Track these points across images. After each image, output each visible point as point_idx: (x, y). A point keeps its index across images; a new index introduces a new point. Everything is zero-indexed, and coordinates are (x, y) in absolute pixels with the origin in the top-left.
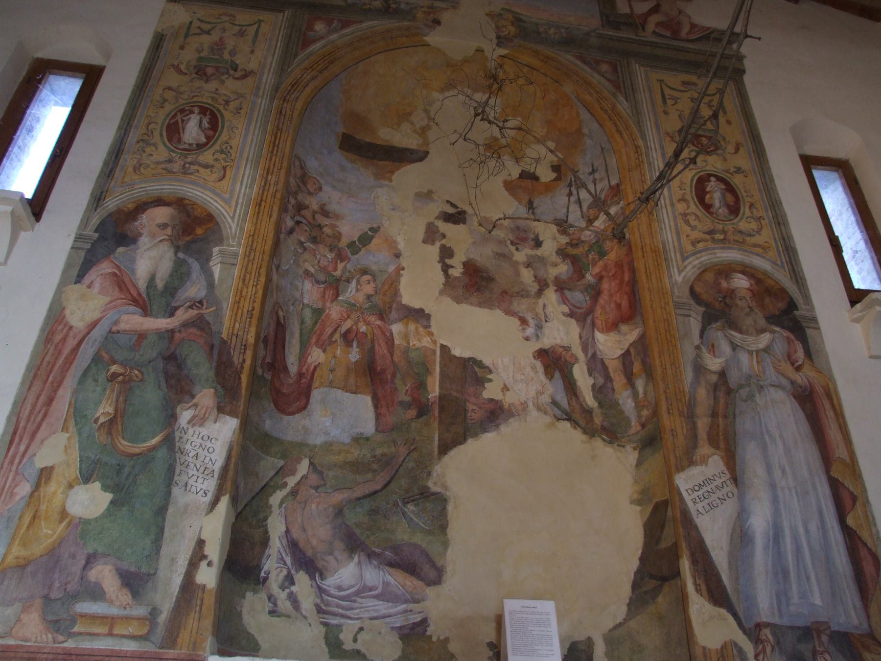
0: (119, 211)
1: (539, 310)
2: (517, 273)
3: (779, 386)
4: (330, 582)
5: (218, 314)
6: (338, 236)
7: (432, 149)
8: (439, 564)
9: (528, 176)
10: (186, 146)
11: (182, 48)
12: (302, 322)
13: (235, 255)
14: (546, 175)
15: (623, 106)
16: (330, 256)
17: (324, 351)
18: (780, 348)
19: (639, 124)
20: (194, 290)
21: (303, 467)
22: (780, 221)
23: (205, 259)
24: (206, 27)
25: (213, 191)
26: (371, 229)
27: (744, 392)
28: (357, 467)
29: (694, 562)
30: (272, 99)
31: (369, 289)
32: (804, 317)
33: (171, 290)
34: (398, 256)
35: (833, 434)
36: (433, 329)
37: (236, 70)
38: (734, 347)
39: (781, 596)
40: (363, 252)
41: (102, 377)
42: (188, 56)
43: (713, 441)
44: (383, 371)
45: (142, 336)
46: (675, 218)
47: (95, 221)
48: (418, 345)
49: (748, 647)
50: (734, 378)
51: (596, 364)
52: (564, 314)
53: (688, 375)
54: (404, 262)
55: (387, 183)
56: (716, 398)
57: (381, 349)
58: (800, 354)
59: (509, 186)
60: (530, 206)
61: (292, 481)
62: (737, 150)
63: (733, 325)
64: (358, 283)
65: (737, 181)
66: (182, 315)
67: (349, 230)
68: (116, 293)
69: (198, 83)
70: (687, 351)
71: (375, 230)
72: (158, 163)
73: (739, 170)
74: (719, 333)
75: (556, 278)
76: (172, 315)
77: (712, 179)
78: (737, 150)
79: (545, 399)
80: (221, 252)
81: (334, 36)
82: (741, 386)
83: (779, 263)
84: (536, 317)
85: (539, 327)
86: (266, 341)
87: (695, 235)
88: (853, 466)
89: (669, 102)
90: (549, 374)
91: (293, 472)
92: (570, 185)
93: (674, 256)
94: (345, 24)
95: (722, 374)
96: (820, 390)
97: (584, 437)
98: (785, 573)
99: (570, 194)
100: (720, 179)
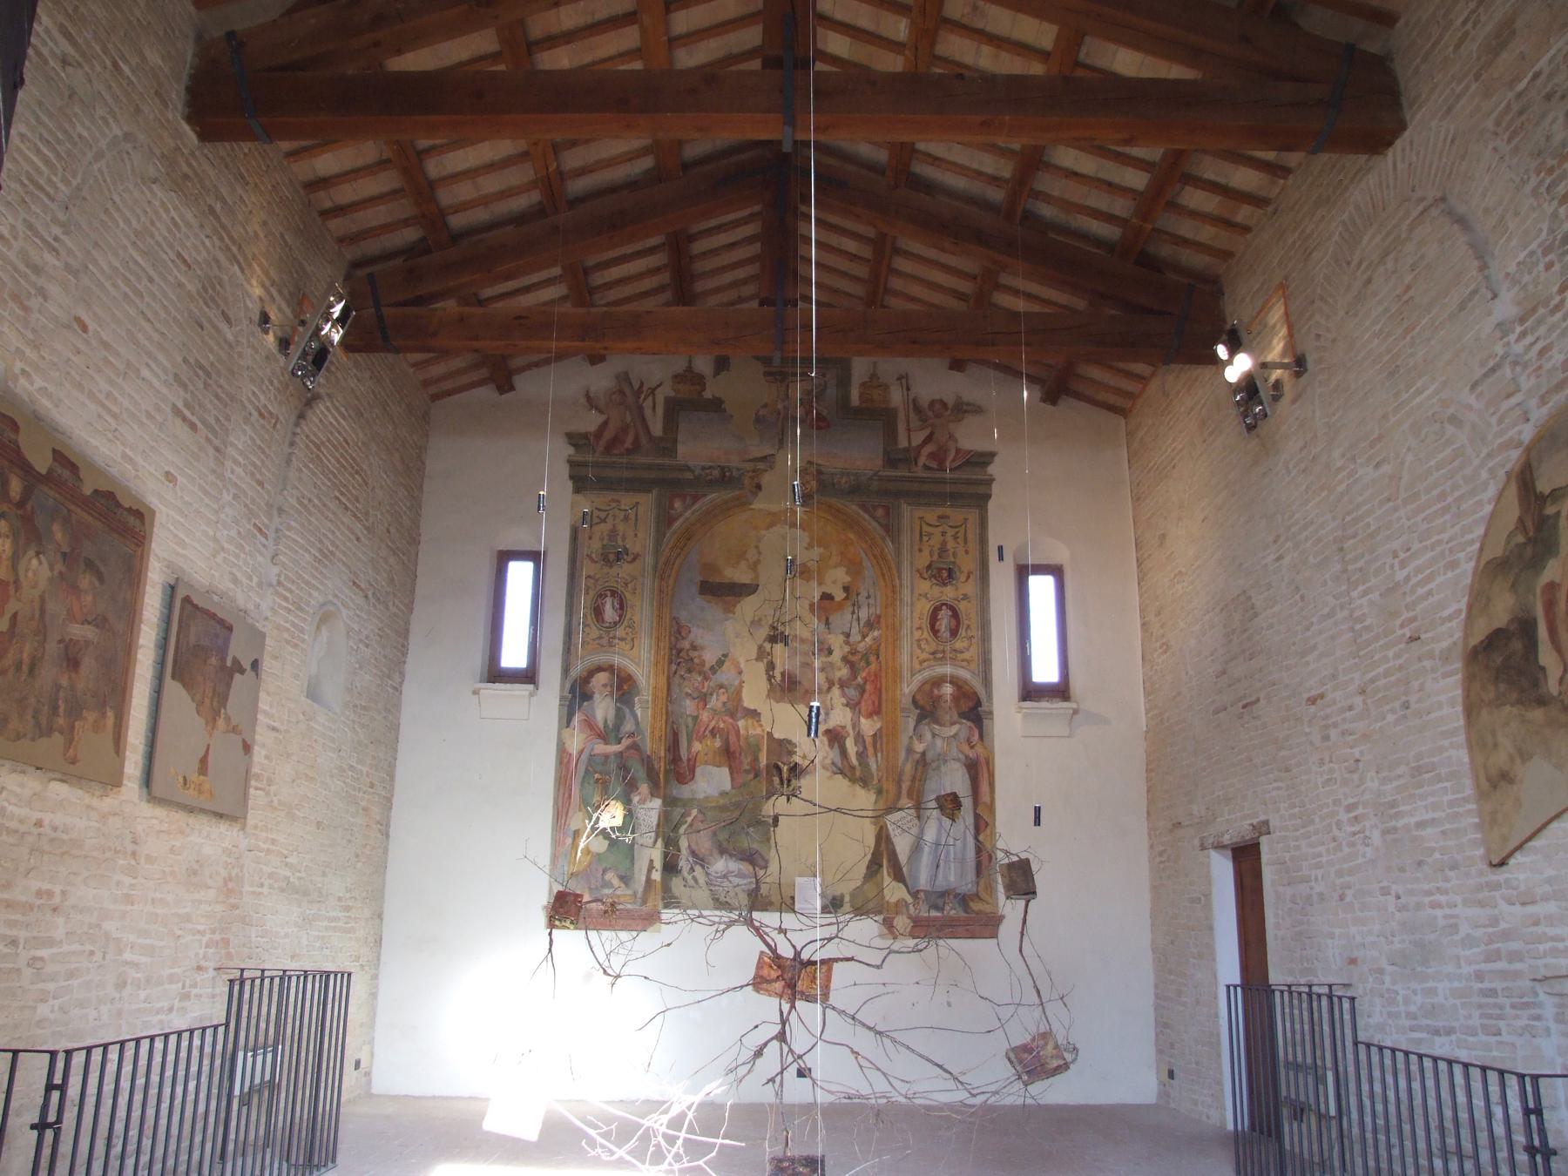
1: (828, 702)
3: (958, 760)
4: (712, 870)
6: (703, 663)
7: (762, 581)
8: (767, 858)
9: (827, 597)
10: (608, 625)
11: (590, 538)
12: (687, 727)
14: (839, 595)
15: (889, 547)
16: (699, 679)
17: (701, 742)
18: (964, 734)
20: (629, 726)
21: (694, 812)
22: (985, 638)
23: (631, 705)
24: (603, 515)
25: (629, 658)
26: (723, 655)
27: (934, 765)
28: (723, 809)
29: (889, 861)
30: (654, 577)
31: (724, 698)
32: (985, 712)
33: (617, 727)
34: (740, 673)
35: (984, 787)
36: (762, 723)
37: (627, 554)
38: (934, 735)
40: (719, 672)
41: (592, 781)
42: (596, 545)
43: (910, 796)
44: (734, 752)
45: (607, 756)
46: (912, 644)
47: (568, 686)
48: (754, 733)
49: (909, 899)
50: (929, 756)
51: (859, 738)
52: (843, 705)
53: (903, 755)
54: (745, 677)
55: (731, 615)
57: (732, 738)
60: (827, 623)
61: (689, 819)
62: (968, 577)
63: (938, 722)
64: (717, 695)
65: (962, 607)
66: (626, 742)
67: (710, 657)
69: (606, 569)
71: (725, 656)
72: (594, 640)
73: (965, 597)
74: (926, 727)
75: (840, 679)
77: (944, 607)
78: (968, 577)
79: (828, 761)
81: (688, 514)
82: (933, 761)
83: (976, 672)
87: (924, 656)
88: (991, 808)
89: (925, 539)
90: (831, 747)
91: (689, 815)
92: (854, 605)
93: (906, 674)
94: (696, 499)
95: (923, 754)
96: (982, 760)
97: (849, 784)
99: (853, 613)
100: (952, 608)
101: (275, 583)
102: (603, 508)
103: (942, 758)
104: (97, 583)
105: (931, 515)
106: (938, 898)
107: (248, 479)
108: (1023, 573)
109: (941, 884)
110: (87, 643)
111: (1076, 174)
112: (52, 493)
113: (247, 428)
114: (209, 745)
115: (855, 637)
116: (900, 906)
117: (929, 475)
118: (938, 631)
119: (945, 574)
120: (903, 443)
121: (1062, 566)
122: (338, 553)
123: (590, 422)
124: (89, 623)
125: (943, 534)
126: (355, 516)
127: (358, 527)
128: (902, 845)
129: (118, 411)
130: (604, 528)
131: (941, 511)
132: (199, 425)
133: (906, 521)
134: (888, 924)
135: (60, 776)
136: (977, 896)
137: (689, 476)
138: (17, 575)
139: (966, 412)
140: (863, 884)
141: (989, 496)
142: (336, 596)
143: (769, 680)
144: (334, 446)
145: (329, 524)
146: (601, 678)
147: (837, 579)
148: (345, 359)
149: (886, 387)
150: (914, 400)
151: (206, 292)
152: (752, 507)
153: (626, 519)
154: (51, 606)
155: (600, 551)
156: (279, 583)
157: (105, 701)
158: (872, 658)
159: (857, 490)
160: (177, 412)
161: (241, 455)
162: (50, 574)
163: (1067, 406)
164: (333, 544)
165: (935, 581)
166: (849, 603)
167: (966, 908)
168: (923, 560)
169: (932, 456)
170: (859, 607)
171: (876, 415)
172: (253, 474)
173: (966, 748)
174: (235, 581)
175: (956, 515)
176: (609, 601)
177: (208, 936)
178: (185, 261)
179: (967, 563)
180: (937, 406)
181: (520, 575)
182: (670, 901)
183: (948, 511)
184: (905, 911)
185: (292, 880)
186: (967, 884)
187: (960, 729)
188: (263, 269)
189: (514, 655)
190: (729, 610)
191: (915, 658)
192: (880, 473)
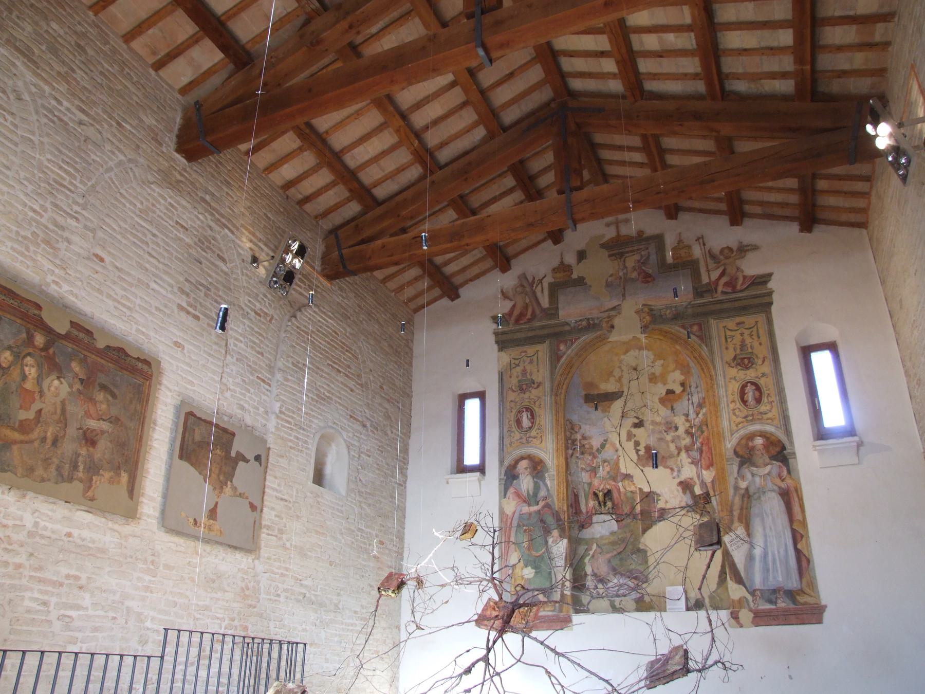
0: (510, 466)
1: (679, 463)
2: (668, 446)
3: (773, 491)
5: (553, 500)
6: (591, 447)
9: (670, 392)
11: (511, 377)
13: (554, 475)
14: (678, 389)
16: (590, 458)
18: (775, 471)
19: (713, 362)
20: (542, 493)
21: (594, 547)
22: (782, 401)
23: (543, 479)
24: (517, 362)
26: (605, 440)
27: (756, 496)
28: (613, 543)
29: (730, 569)
30: (551, 396)
31: (608, 469)
32: (789, 453)
33: (535, 494)
34: (617, 451)
35: (796, 509)
38: (753, 475)
39: (765, 579)
42: (514, 381)
43: (740, 520)
45: (530, 514)
46: (729, 413)
47: (503, 472)
49: (750, 598)
50: (752, 490)
52: (689, 463)
53: (731, 491)
56: (743, 501)
58: (785, 473)
59: (662, 401)
60: (672, 409)
61: (591, 553)
62: (763, 361)
65: (762, 382)
66: (541, 504)
67: (596, 443)
68: (518, 500)
69: (522, 395)
70: (731, 480)
71: (606, 441)
73: (763, 375)
74: (747, 470)
76: (538, 504)
77: (749, 384)
78: (763, 361)
80: (549, 475)
81: (570, 351)
82: (755, 494)
84: (678, 467)
85: (679, 471)
86: (571, 506)
87: (739, 420)
88: (804, 523)
89: (729, 340)
90: (684, 492)
93: (727, 434)
95: (747, 489)
96: (792, 489)
98: (768, 570)
99: (689, 400)
100: (753, 383)
101: (278, 412)
102: (517, 357)
103: (762, 491)
104: (110, 398)
105: (731, 323)
106: (773, 594)
107: (249, 350)
108: (806, 352)
109: (772, 583)
110: (103, 432)
111: (745, 50)
112: (70, 345)
113: (246, 322)
114: (217, 503)
115: (692, 416)
116: (741, 602)
117: (728, 297)
118: (747, 401)
119: (746, 361)
120: (705, 280)
121: (835, 342)
122: (333, 397)
123: (503, 307)
124: (104, 420)
125: (742, 334)
126: (347, 376)
127: (351, 384)
128: (739, 557)
129: (132, 306)
130: (519, 369)
131: (738, 319)
132: (201, 316)
133: (714, 332)
134: (735, 616)
135: (86, 508)
136: (802, 592)
137: (567, 328)
138: (41, 387)
139: (748, 250)
140: (716, 589)
141: (771, 303)
142: (335, 423)
143: (637, 453)
144: (323, 334)
145: (324, 380)
146: (524, 464)
147: (675, 379)
148: (329, 285)
149: (689, 247)
150: (709, 251)
151: (203, 244)
152: (610, 340)
153: (531, 362)
154: (70, 408)
155: (517, 385)
156: (281, 412)
157: (119, 467)
158: (704, 428)
159: (677, 317)
160: (181, 308)
161: (241, 335)
162: (69, 390)
163: (820, 233)
164: (329, 392)
165: (740, 368)
166: (686, 393)
167: (794, 601)
168: (730, 354)
169: (726, 284)
170: (692, 395)
171: (686, 265)
172: (252, 347)
173: (778, 481)
174: (242, 408)
175: (749, 320)
176: (525, 414)
177: (227, 622)
178: (182, 226)
179: (762, 351)
180: (726, 251)
181: (472, 407)
182: (580, 608)
183: (742, 319)
184: (747, 606)
185: (308, 595)
186: (793, 583)
187: (773, 468)
188: (250, 232)
189: (472, 457)
190: (606, 410)
191: (732, 422)
192: (693, 303)
